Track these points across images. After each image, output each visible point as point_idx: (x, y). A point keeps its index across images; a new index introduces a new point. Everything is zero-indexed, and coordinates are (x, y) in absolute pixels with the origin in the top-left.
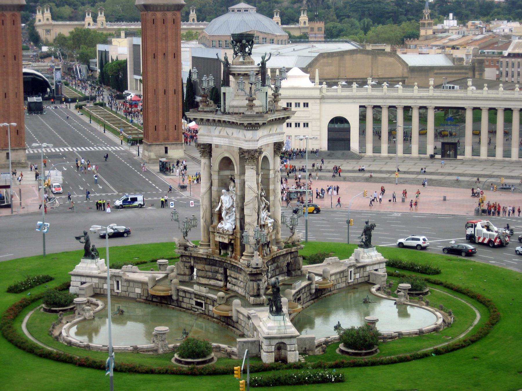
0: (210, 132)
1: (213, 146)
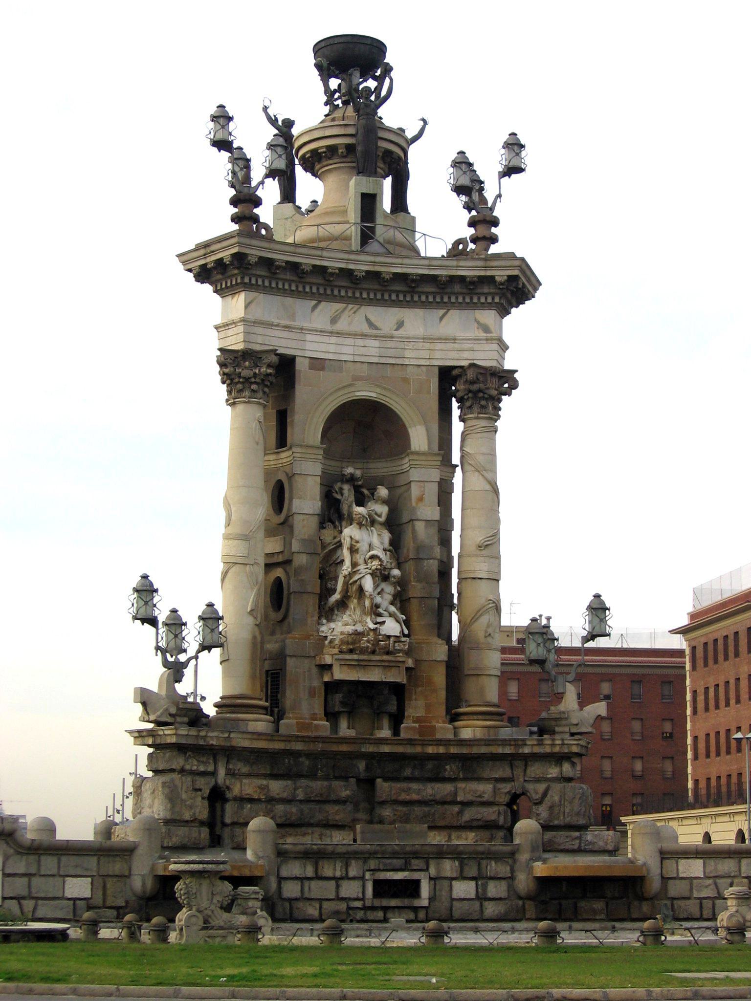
0: (293, 317)
1: (301, 366)
